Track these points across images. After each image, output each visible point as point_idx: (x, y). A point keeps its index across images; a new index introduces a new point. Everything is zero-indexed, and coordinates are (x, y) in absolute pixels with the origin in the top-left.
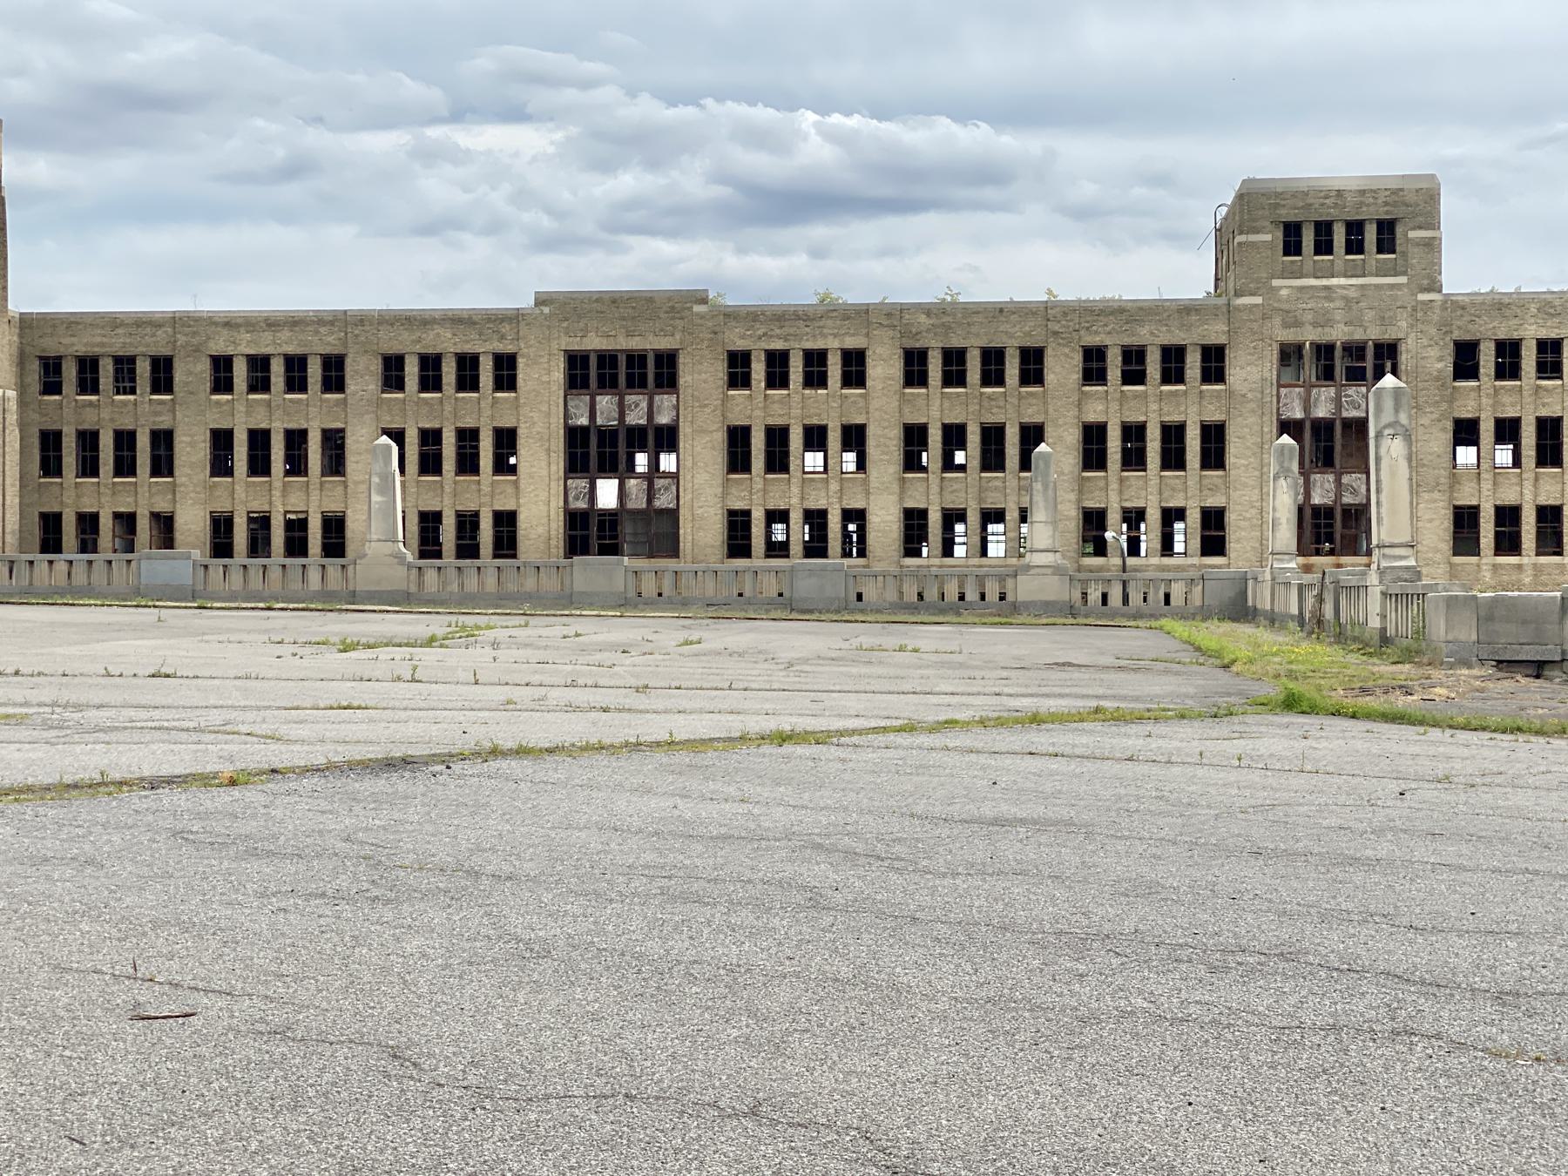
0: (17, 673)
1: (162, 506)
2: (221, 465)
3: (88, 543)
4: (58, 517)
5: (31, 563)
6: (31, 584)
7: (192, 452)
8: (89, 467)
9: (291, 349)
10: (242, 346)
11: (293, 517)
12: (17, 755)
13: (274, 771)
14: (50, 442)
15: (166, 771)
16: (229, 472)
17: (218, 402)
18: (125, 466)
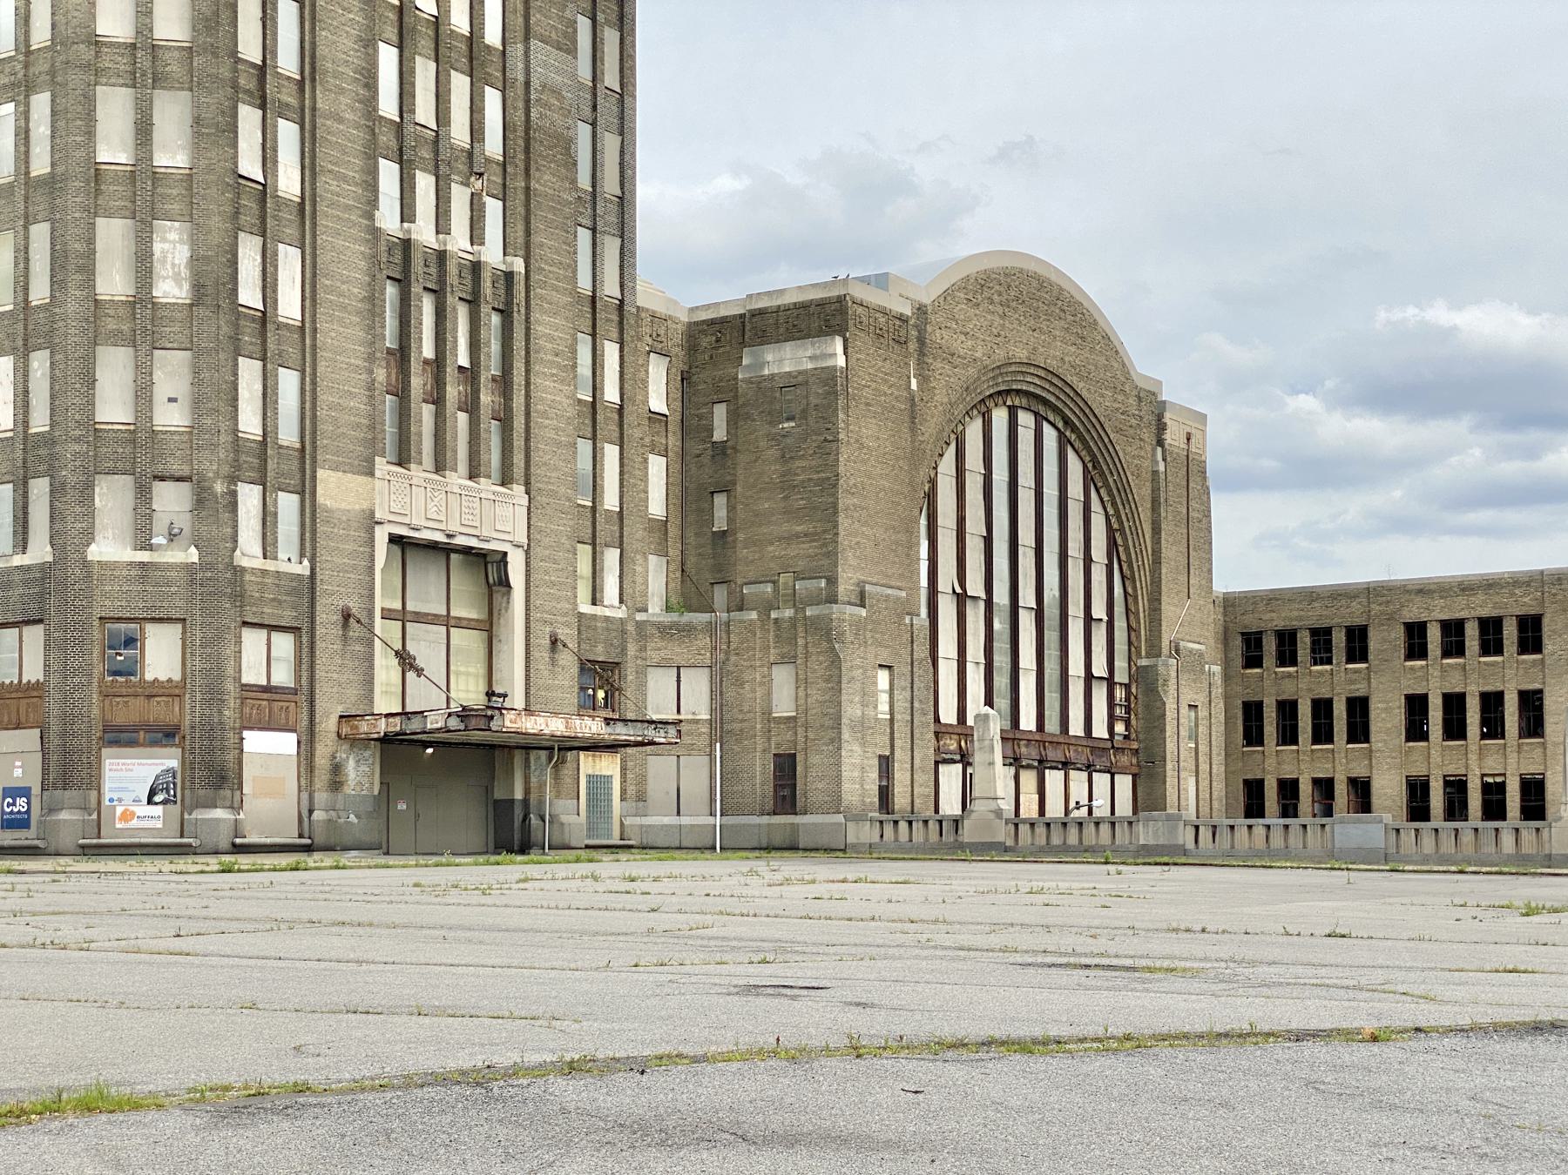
0: (1203, 930)
1: (1359, 771)
2: (1416, 731)
3: (1289, 808)
4: (1260, 784)
5: (1232, 827)
6: (1233, 847)
7: (1387, 718)
8: (1288, 735)
9: (1487, 612)
10: (1436, 612)
11: (1490, 780)
12: (1183, 1004)
13: (1418, 1030)
14: (1253, 712)
15: (1314, 1025)
16: (1424, 737)
17: (1412, 668)
18: (1323, 734)
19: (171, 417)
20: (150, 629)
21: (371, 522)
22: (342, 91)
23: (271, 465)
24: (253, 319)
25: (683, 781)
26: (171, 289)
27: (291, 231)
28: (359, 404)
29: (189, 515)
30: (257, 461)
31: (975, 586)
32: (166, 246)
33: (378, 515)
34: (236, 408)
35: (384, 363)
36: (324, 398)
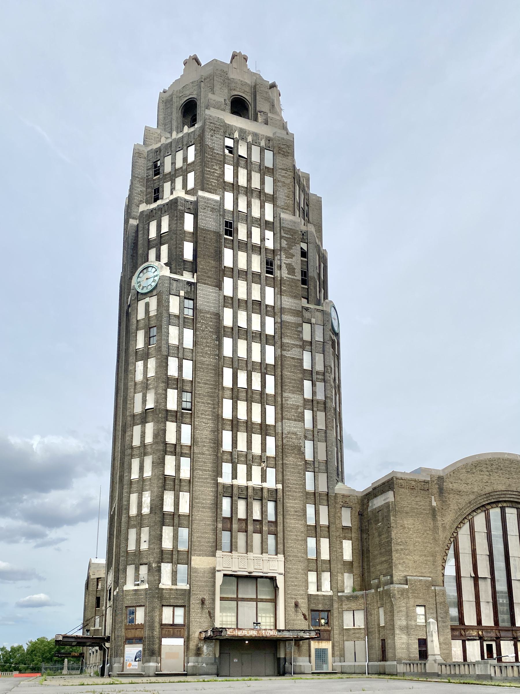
19: (144, 546)
20: (137, 608)
21: (213, 572)
22: (205, 446)
23: (175, 557)
24: (170, 515)
25: (358, 651)
26: (146, 510)
27: (186, 488)
28: (210, 536)
29: (147, 575)
30: (175, 557)
31: (484, 571)
32: (146, 498)
33: (217, 569)
34: (161, 542)
35: (221, 522)
36: (195, 535)
